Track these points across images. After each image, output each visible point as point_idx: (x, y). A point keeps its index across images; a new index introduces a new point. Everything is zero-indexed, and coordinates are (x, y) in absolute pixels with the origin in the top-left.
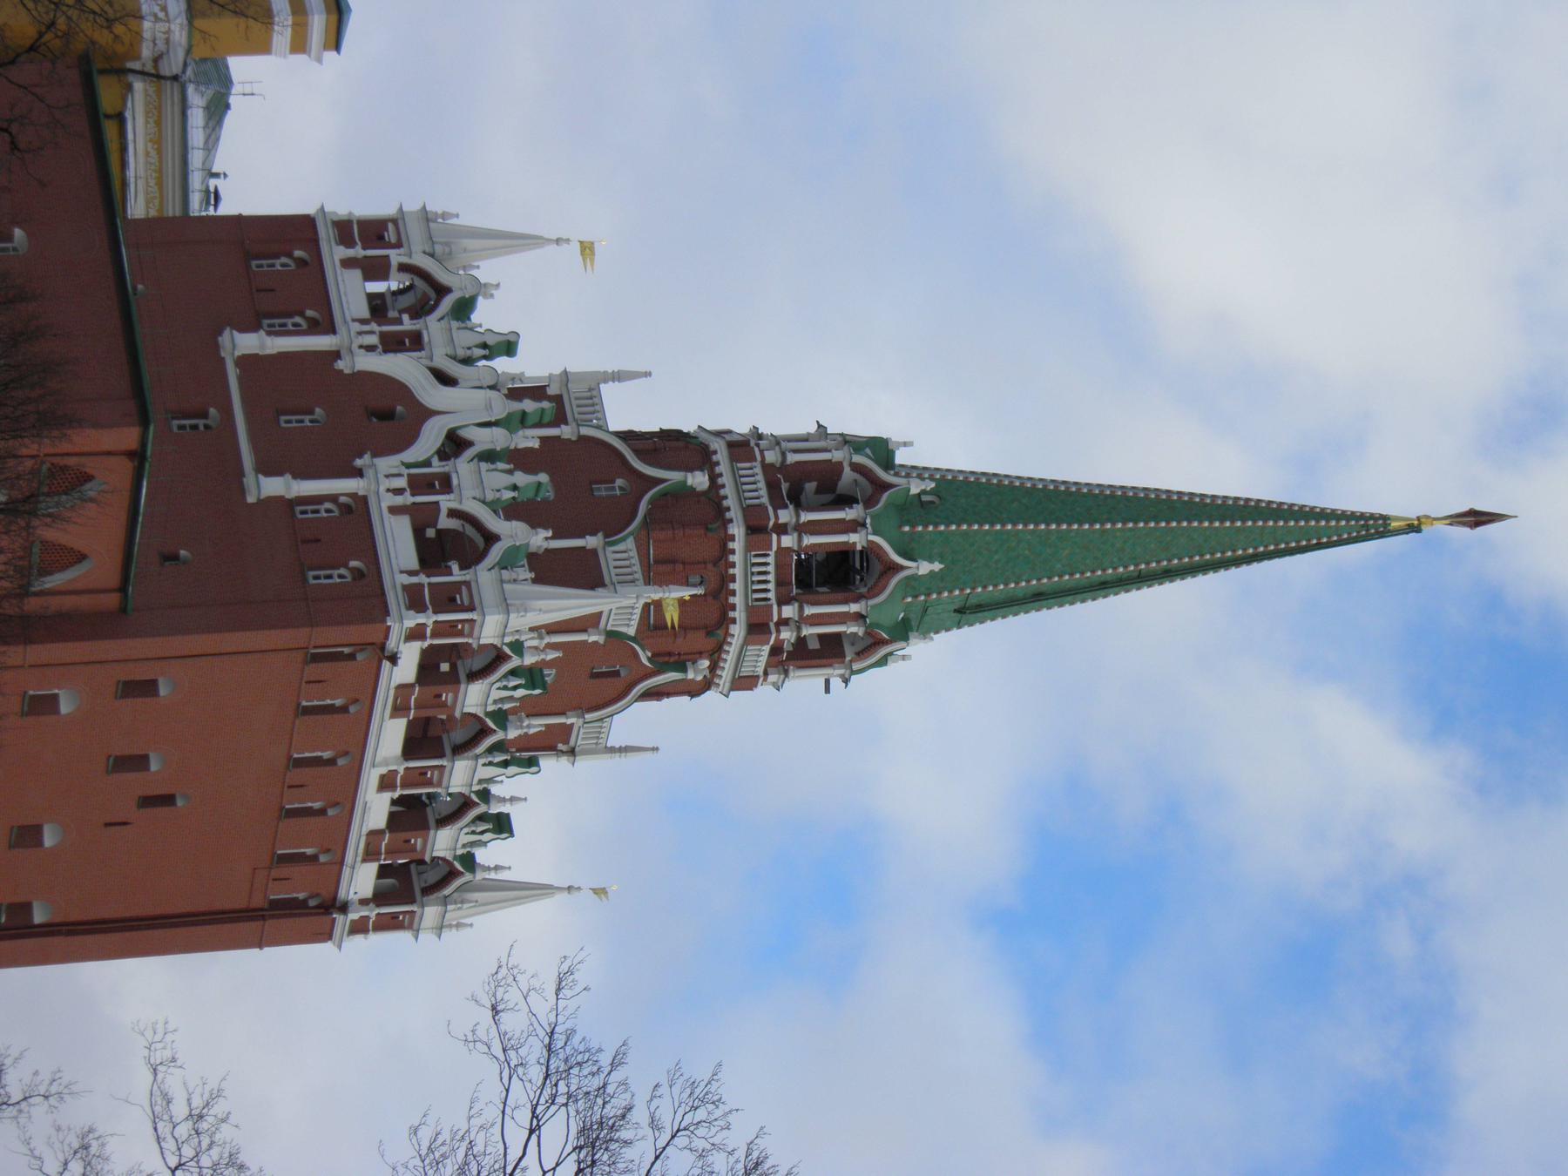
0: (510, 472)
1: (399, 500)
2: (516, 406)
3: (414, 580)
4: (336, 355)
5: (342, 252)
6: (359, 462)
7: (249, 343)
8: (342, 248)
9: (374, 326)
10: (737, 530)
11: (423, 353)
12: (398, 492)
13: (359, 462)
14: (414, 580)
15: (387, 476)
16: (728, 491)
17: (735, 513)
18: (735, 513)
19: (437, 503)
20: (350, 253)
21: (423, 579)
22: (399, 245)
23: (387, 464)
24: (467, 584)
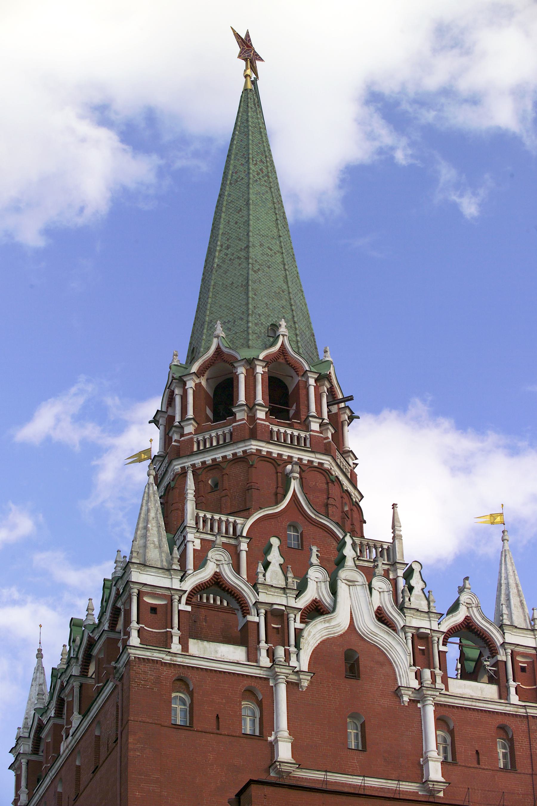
0: (411, 589)
1: (439, 680)
2: (349, 562)
3: (513, 690)
4: (292, 686)
5: (176, 647)
6: (406, 699)
7: (285, 752)
8: (173, 645)
9: (263, 644)
10: (327, 462)
11: (292, 616)
12: (433, 676)
13: (406, 699)
14: (513, 690)
15: (421, 683)
16: (296, 455)
17: (317, 459)
18: (317, 459)
19: (439, 652)
20: (176, 640)
21: (512, 685)
22: (171, 600)
23: (407, 678)
24: (513, 654)
